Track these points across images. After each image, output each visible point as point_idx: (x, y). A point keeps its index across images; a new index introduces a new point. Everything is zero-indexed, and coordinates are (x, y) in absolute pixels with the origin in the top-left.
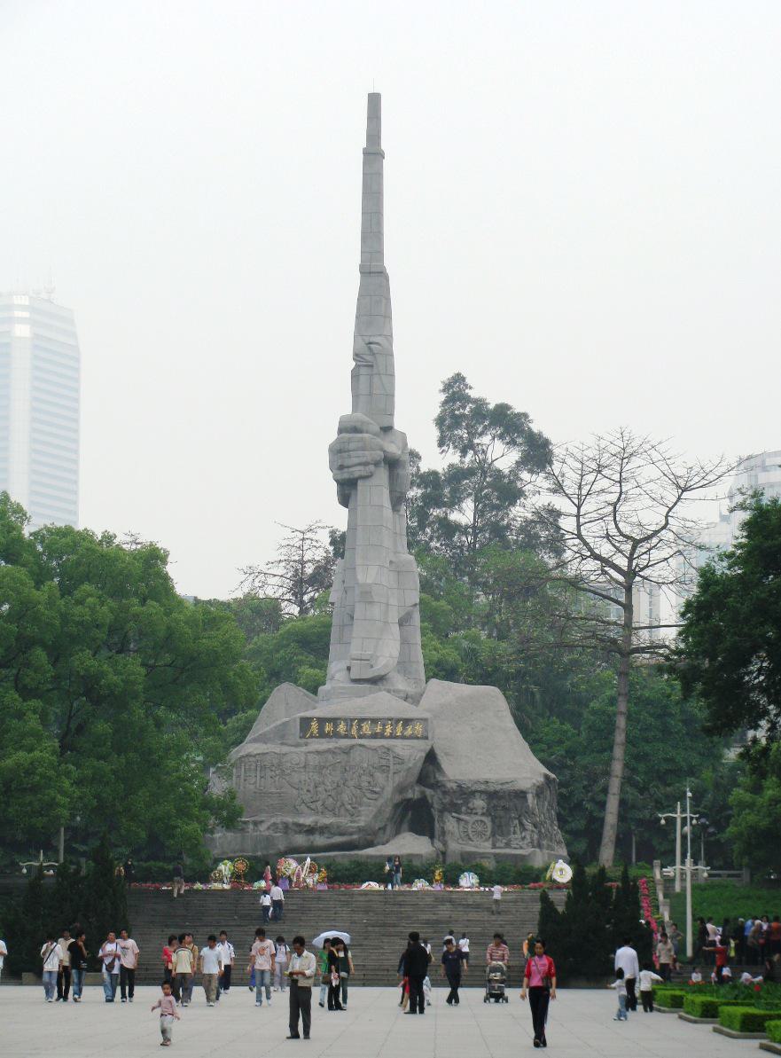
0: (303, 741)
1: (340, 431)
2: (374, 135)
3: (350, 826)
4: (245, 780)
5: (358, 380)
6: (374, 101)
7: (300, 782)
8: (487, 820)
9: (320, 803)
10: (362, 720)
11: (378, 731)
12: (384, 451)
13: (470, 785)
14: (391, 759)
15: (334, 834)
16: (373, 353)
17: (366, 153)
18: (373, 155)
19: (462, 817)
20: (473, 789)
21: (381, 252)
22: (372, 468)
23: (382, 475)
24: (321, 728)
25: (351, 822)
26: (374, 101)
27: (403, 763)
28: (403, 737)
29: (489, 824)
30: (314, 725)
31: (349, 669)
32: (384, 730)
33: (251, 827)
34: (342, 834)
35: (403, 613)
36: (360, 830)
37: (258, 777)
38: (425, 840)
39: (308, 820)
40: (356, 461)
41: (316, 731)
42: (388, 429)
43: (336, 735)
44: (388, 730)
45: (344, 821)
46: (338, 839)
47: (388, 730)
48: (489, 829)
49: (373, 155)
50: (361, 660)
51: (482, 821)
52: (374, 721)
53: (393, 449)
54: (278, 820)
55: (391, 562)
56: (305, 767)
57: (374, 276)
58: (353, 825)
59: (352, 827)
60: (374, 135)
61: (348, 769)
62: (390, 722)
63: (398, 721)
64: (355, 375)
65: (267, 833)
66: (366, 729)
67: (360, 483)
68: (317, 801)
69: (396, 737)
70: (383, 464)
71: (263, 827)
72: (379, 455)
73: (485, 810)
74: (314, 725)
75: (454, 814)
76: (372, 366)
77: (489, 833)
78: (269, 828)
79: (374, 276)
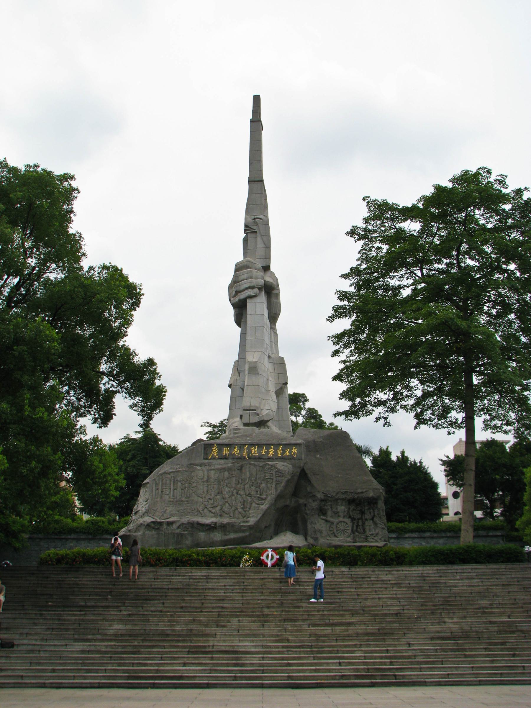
0: (206, 461)
1: (236, 270)
3: (242, 526)
4: (162, 492)
5: (247, 243)
6: (257, 100)
7: (204, 492)
8: (348, 521)
9: (219, 508)
10: (252, 445)
11: (264, 453)
12: (265, 281)
13: (334, 494)
14: (274, 473)
16: (256, 224)
17: (252, 121)
18: (256, 123)
19: (329, 519)
20: (337, 497)
21: (261, 171)
22: (256, 290)
23: (263, 298)
24: (220, 450)
25: (244, 522)
26: (257, 100)
27: (283, 476)
28: (283, 459)
29: (350, 524)
30: (215, 450)
31: (241, 417)
32: (268, 453)
33: (165, 526)
34: (236, 532)
35: (278, 388)
36: (251, 527)
39: (208, 520)
40: (246, 286)
41: (216, 454)
44: (271, 452)
45: (237, 520)
46: (232, 536)
47: (271, 452)
48: (350, 528)
49: (256, 123)
50: (250, 410)
51: (344, 522)
53: (268, 279)
54: (185, 520)
55: (269, 357)
56: (207, 481)
57: (256, 181)
58: (244, 524)
59: (245, 526)
61: (240, 481)
62: (272, 447)
63: (280, 444)
64: (245, 241)
65: (178, 531)
66: (255, 452)
67: (248, 301)
68: (217, 506)
69: (278, 459)
71: (175, 526)
72: (261, 282)
73: (345, 513)
74: (215, 450)
75: (322, 517)
76: (256, 232)
77: (349, 531)
78: (178, 528)
79: (256, 181)
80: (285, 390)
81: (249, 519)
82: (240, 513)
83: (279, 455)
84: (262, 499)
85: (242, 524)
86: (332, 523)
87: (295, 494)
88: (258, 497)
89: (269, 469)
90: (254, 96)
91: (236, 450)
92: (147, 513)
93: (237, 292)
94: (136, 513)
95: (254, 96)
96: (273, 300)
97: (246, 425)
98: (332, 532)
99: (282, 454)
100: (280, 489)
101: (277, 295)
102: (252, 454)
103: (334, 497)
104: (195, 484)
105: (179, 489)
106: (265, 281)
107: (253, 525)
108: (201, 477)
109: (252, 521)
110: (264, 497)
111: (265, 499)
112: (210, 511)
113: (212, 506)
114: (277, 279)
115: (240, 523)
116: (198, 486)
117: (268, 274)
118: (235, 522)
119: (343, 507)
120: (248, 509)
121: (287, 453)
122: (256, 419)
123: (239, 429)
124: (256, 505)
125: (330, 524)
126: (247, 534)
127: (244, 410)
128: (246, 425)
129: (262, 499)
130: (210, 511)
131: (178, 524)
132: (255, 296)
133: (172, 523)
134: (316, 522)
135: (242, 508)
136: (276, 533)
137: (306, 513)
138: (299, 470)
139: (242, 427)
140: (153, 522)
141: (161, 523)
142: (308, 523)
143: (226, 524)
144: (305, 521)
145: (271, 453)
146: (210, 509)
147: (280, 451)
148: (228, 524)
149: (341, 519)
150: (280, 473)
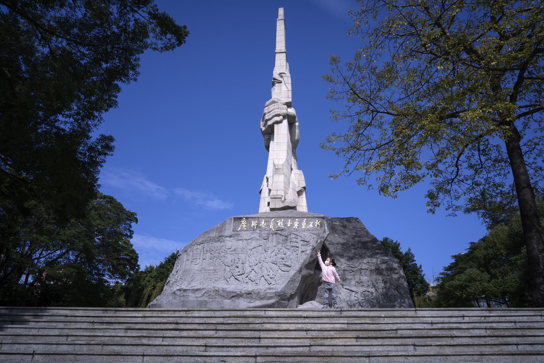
0: (236, 233)
15: (255, 299)
22: (281, 117)
25: (270, 289)
31: (269, 203)
59: (271, 293)
86: (357, 293)
91: (263, 223)
104: (223, 254)
108: (229, 247)
112: (236, 279)
113: (239, 274)
116: (226, 255)
122: (281, 205)
128: (272, 210)
131: (204, 291)
132: (280, 122)
134: (341, 292)
146: (236, 277)
147: (304, 224)
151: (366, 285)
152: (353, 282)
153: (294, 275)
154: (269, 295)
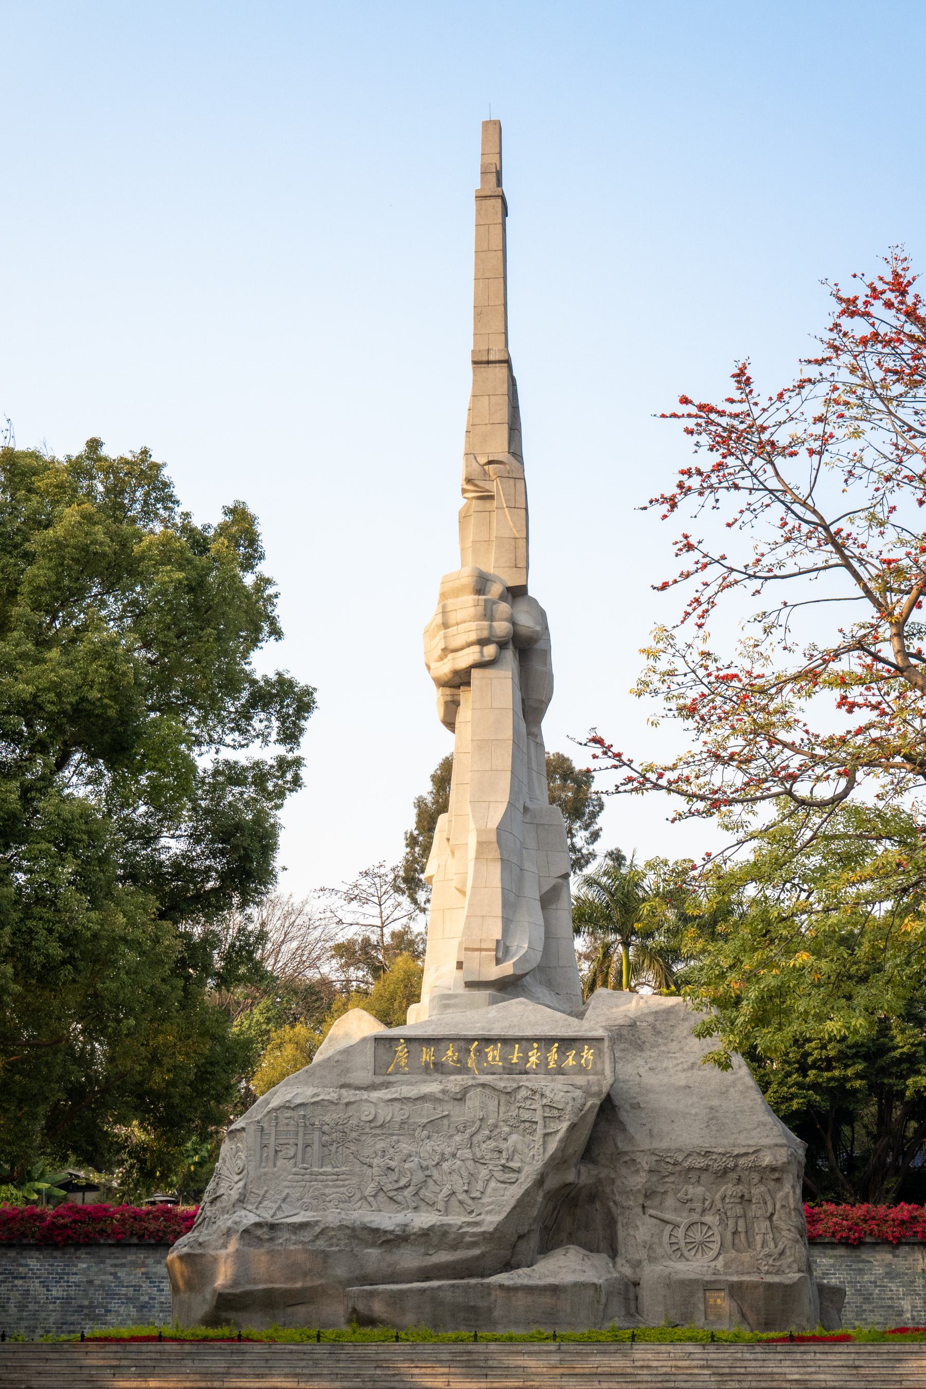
1: (444, 596)
2: (494, 174)
4: (276, 1151)
6: (493, 131)
11: (515, 1060)
13: (680, 1159)
15: (438, 1248)
19: (667, 1216)
20: (686, 1164)
26: (493, 131)
28: (560, 1071)
31: (460, 965)
34: (454, 1247)
36: (487, 1237)
37: (300, 1146)
38: (601, 1259)
42: (517, 593)
43: (439, 1068)
46: (443, 1257)
48: (717, 1238)
50: (480, 950)
52: (507, 1041)
53: (526, 621)
55: (526, 809)
57: (494, 363)
59: (474, 1235)
60: (494, 174)
62: (535, 1045)
66: (494, 1057)
67: (475, 673)
68: (406, 1187)
70: (511, 646)
79: (494, 363)
80: (565, 889)
81: (482, 1217)
82: (461, 1202)
83: (552, 1065)
84: (513, 1170)
85: (464, 1230)
86: (676, 1226)
87: (588, 1154)
88: (503, 1166)
89: (527, 1098)
90: (486, 125)
91: (450, 1053)
92: (242, 1200)
93: (446, 651)
94: (212, 1202)
95: (486, 125)
96: (537, 666)
97: (470, 985)
98: (675, 1247)
99: (559, 1062)
100: (553, 1146)
101: (546, 654)
102: (487, 1062)
103: (680, 1164)
104: (354, 1134)
105: (316, 1146)
106: (514, 624)
107: (491, 1233)
108: (370, 1118)
109: (491, 1220)
110: (514, 1165)
111: (519, 1171)
112: (391, 1198)
114: (543, 614)
115: (461, 1227)
117: (522, 606)
118: (450, 1225)
119: (700, 1190)
120: (477, 1194)
121: (570, 1062)
123: (455, 996)
124: (499, 1185)
125: (669, 1227)
126: (476, 1252)
127: (467, 949)
128: (470, 985)
129: (513, 1170)
130: (391, 1198)
131: (318, 1229)
133: (303, 1226)
134: (639, 1223)
135: (466, 1191)
136: (546, 1249)
137: (615, 1202)
138: (595, 1101)
139: (461, 990)
140: (258, 1225)
141: (273, 1227)
142: (619, 1226)
143: (428, 1229)
144: (611, 1223)
145: (533, 1059)
146: (391, 1194)
148: (431, 1228)
149: (695, 1217)
150: (553, 1111)
151: (699, 1210)
152: (670, 1201)
153: (527, 1193)
154: (468, 1239)
